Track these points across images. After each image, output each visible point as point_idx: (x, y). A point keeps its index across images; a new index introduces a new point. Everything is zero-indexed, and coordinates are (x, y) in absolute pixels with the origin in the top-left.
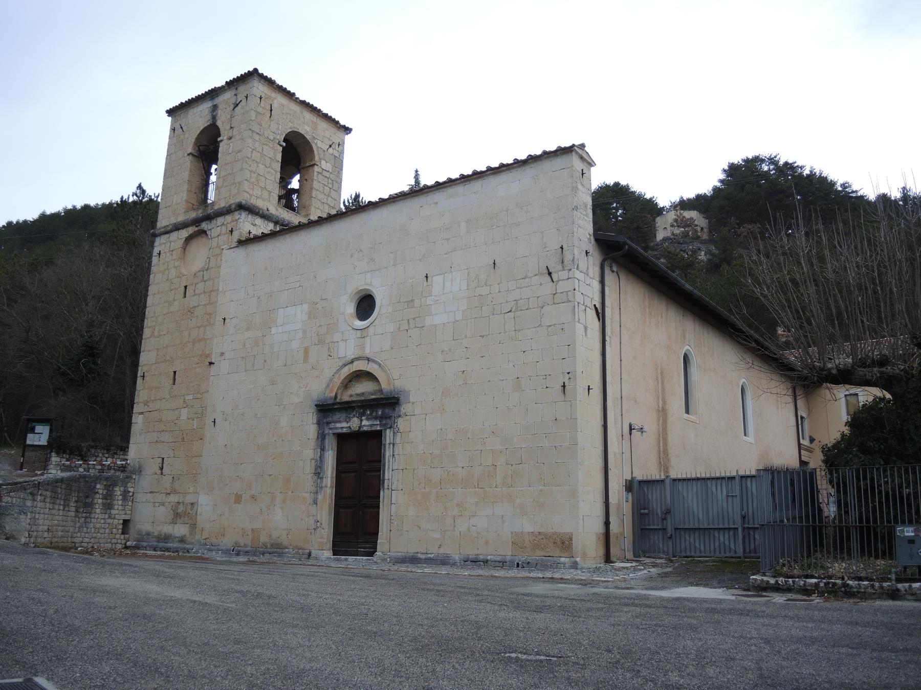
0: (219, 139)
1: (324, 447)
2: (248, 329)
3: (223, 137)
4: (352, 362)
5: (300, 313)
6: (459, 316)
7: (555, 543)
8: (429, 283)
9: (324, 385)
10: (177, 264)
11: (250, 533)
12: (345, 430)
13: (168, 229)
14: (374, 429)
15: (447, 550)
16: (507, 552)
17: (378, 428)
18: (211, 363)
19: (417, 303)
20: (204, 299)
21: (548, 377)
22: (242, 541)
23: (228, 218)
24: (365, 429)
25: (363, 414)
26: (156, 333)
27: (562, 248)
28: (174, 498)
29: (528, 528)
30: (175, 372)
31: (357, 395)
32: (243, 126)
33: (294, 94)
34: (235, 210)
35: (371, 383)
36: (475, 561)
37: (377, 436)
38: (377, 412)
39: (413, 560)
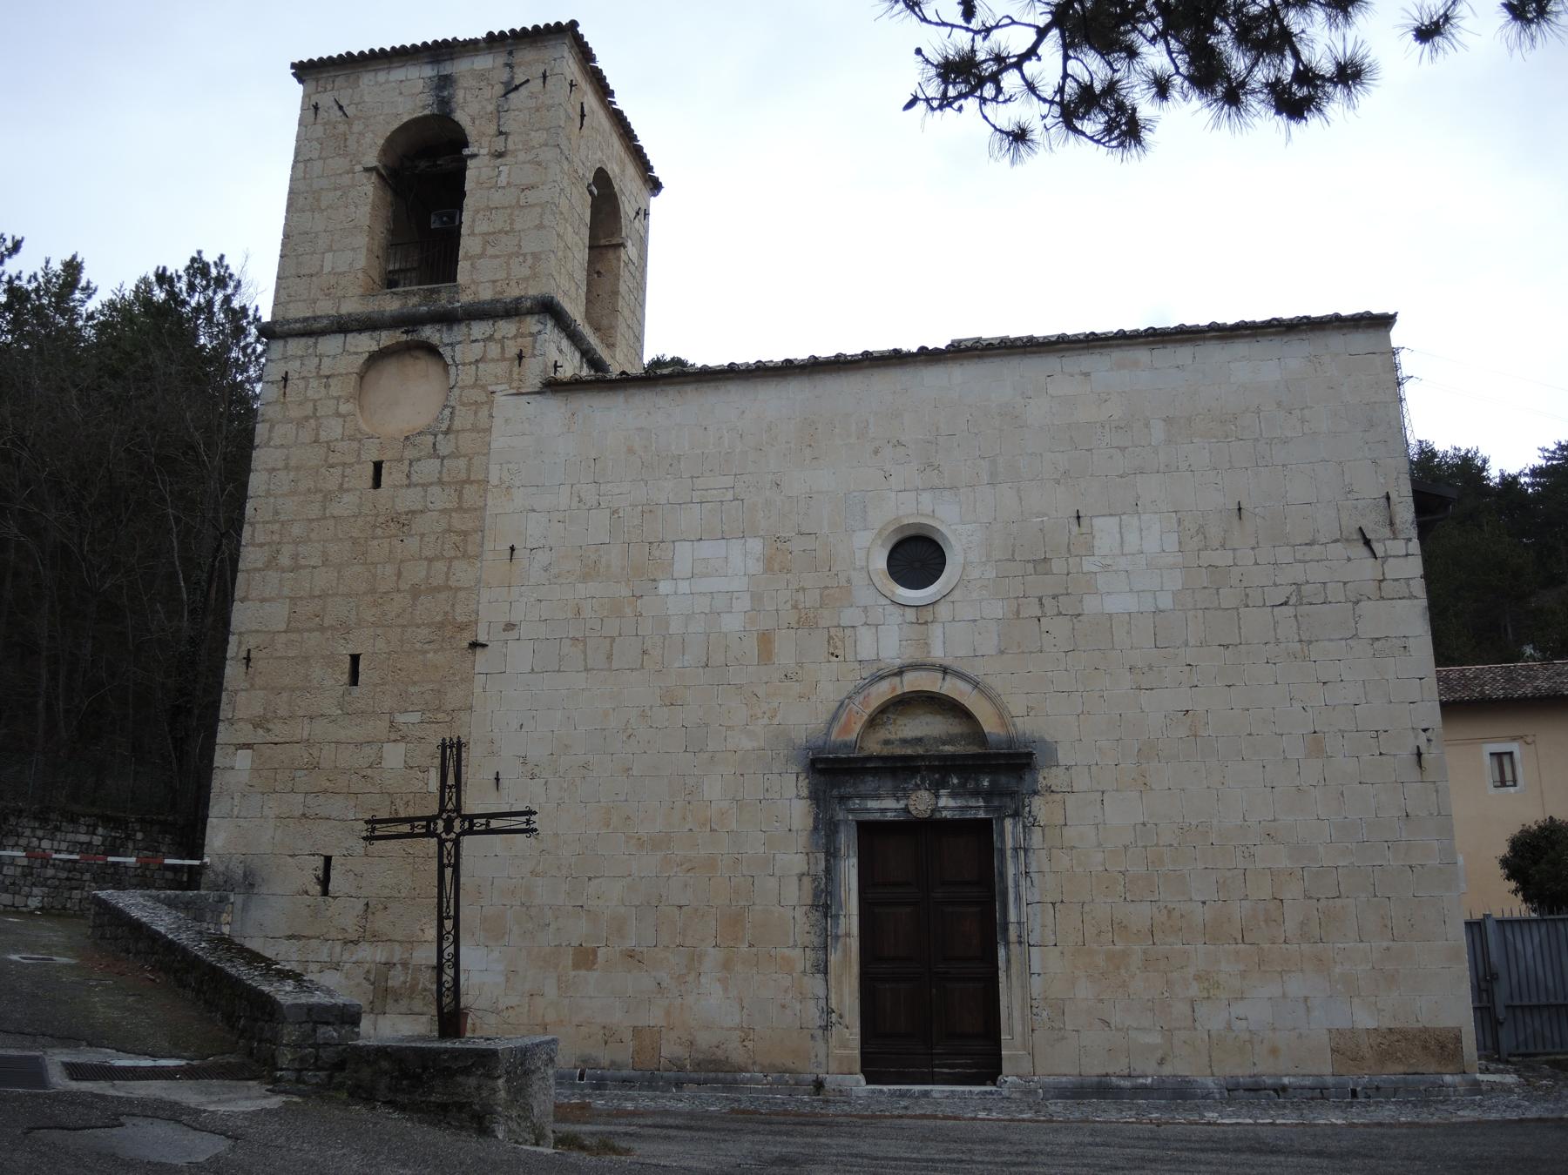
0: (466, 152)
1: (837, 850)
2: (585, 578)
3: (479, 144)
4: (900, 672)
5: (741, 560)
6: (1166, 602)
7: (1425, 1048)
8: (1083, 530)
9: (825, 717)
10: (344, 408)
11: (628, 1036)
12: (890, 816)
13: (316, 326)
14: (969, 815)
15: (1181, 1067)
16: (1324, 1067)
17: (982, 815)
18: (475, 645)
19: (1057, 566)
20: (440, 498)
21: (1383, 736)
22: (604, 1056)
23: (506, 328)
24: (946, 814)
25: (942, 784)
26: (285, 561)
27: (1388, 498)
28: (371, 954)
29: (1365, 1020)
30: (355, 659)
31: (905, 741)
32: (538, 138)
33: (612, 93)
34: (530, 312)
35: (939, 718)
36: (1255, 1089)
37: (981, 834)
38: (977, 780)
39: (1103, 1090)
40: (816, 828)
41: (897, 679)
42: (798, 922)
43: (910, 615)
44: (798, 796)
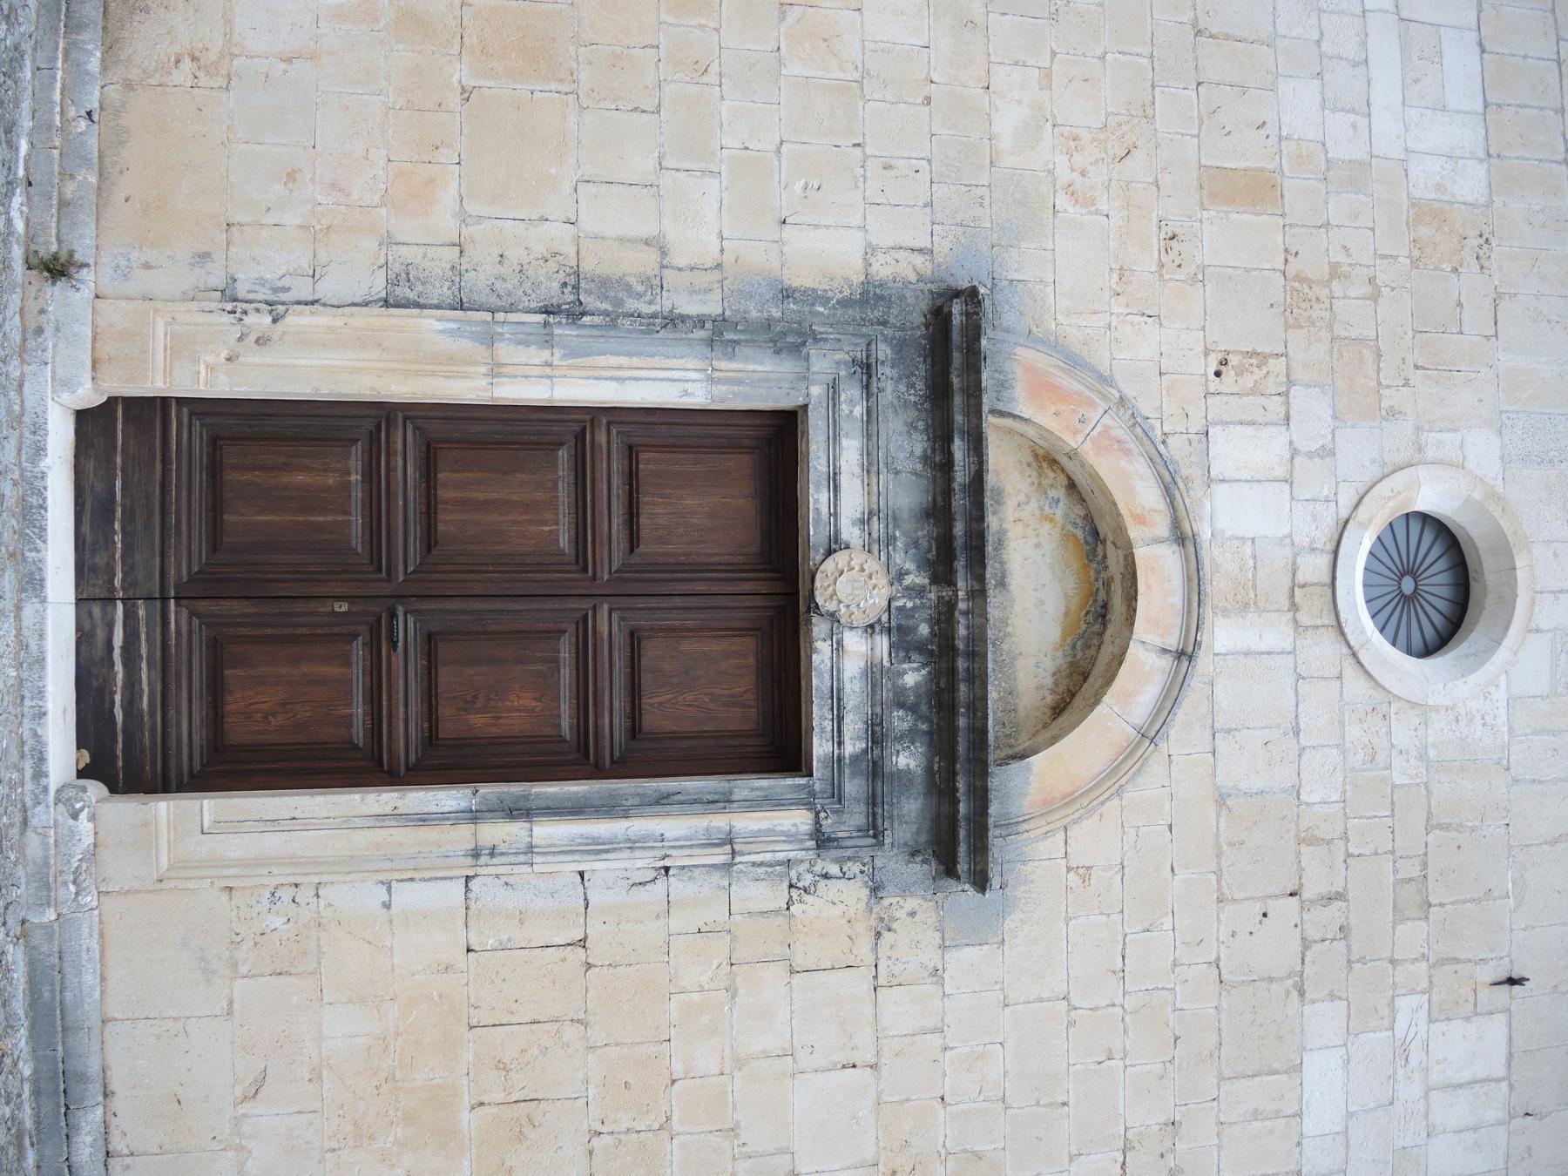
4: (1182, 537)
8: (1484, 993)
12: (817, 499)
14: (820, 716)
17: (820, 748)
19: (1413, 935)
35: (1054, 633)
37: (778, 745)
38: (911, 735)
40: (787, 294)
41: (1163, 528)
42: (529, 236)
43: (1314, 568)
44: (871, 250)
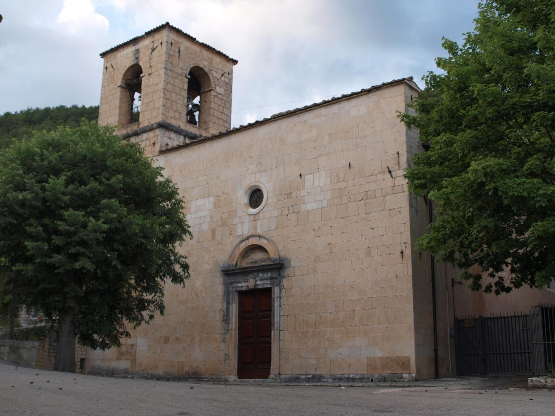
0: (141, 75)
1: (229, 301)
3: (145, 72)
4: (248, 238)
6: (325, 204)
7: (398, 364)
8: (302, 180)
9: (228, 256)
12: (244, 289)
14: (265, 286)
16: (364, 371)
17: (269, 286)
19: (294, 195)
21: (391, 247)
23: (151, 134)
24: (259, 287)
27: (398, 153)
29: (379, 354)
33: (195, 39)
34: (156, 128)
37: (268, 292)
40: (224, 294)
41: (247, 241)
43: (252, 217)
44: (220, 284)
